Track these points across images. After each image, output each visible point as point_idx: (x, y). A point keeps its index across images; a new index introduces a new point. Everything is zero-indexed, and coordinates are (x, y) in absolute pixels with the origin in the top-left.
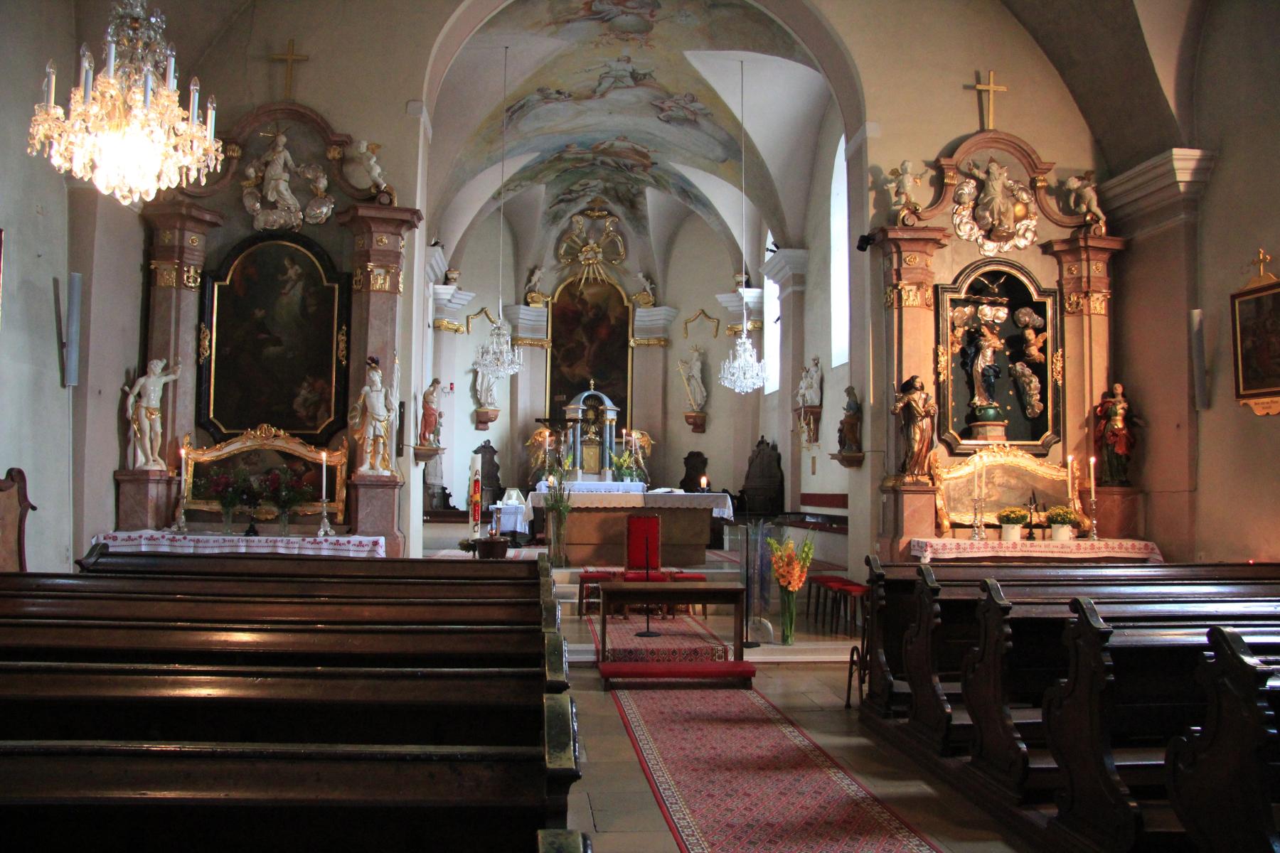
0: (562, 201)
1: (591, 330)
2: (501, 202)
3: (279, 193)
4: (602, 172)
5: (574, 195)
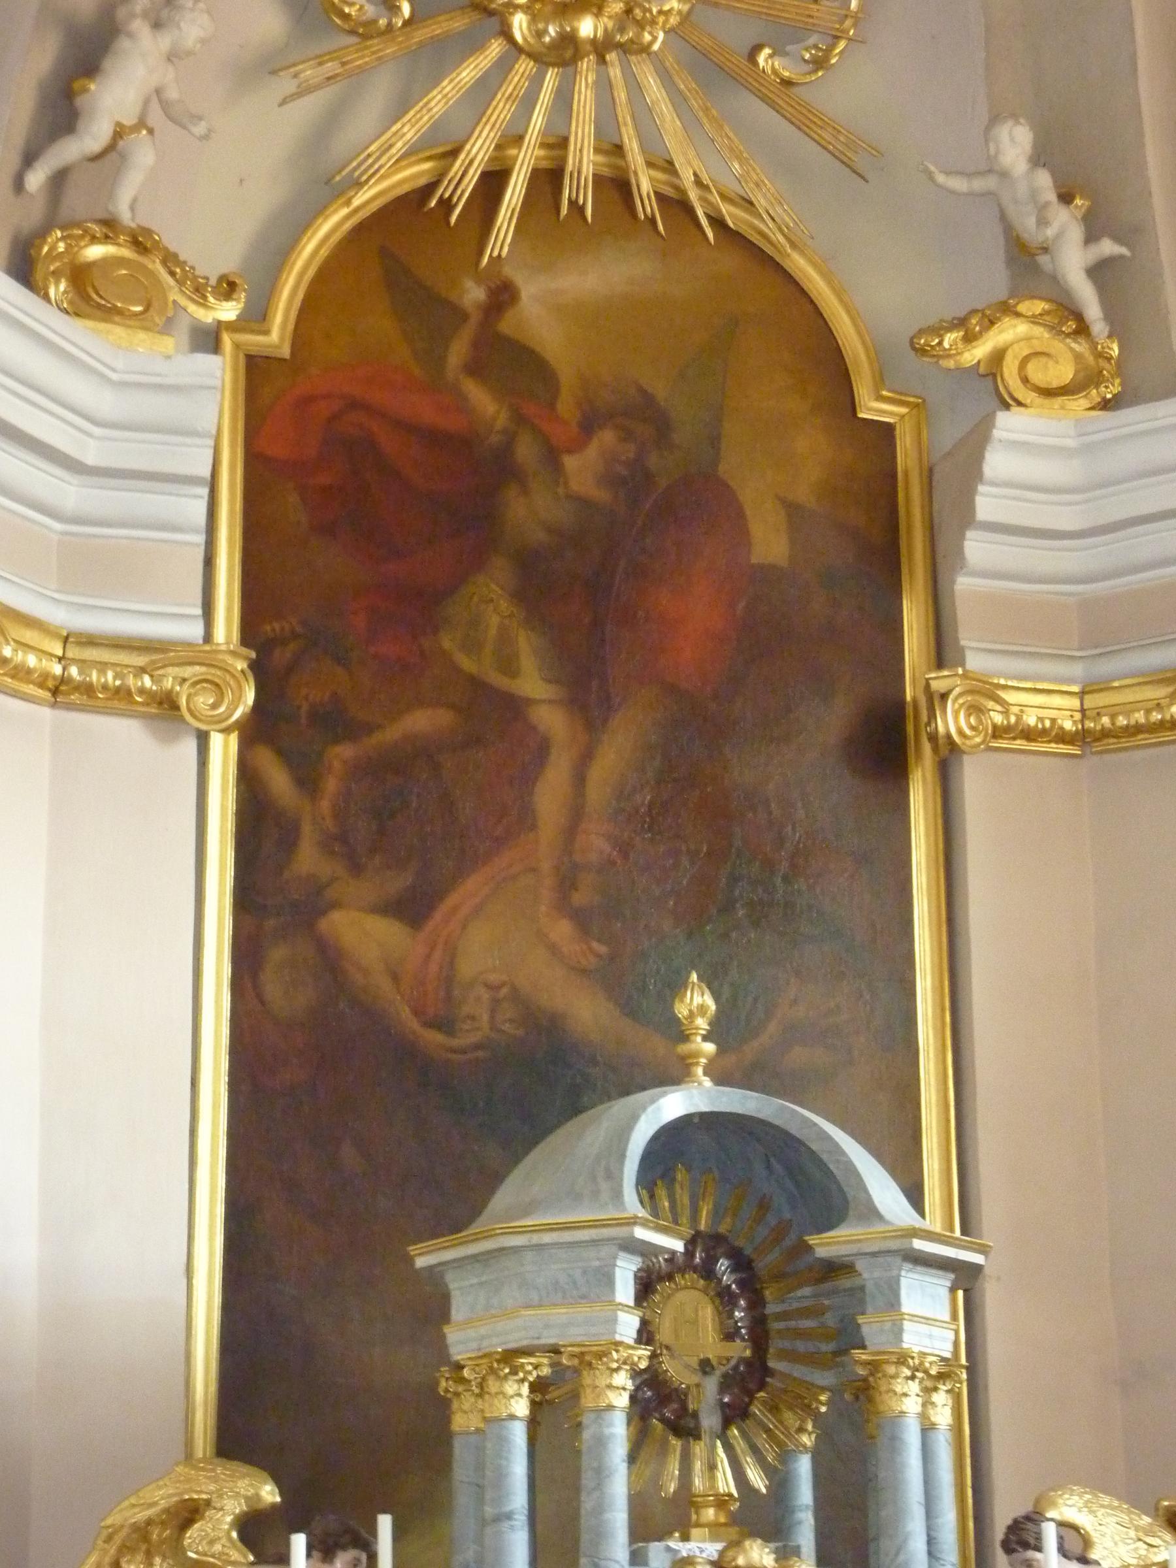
1: (589, 596)
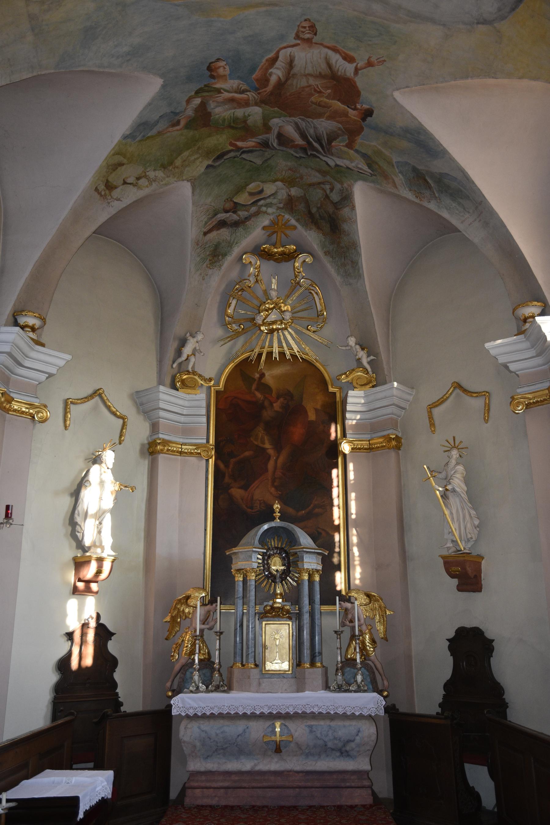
0: (222, 224)
1: (279, 428)
4: (282, 164)
5: (243, 214)
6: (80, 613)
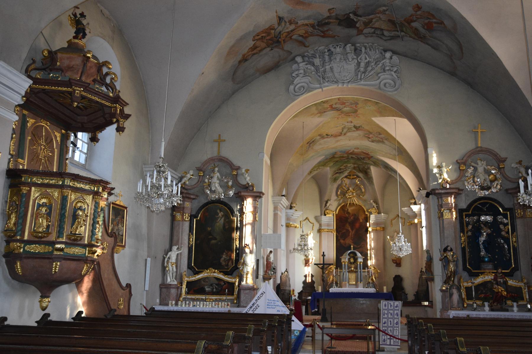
1: (352, 224)
2: (312, 175)
3: (216, 187)
4: (352, 161)
5: (342, 170)
6: (308, 270)
